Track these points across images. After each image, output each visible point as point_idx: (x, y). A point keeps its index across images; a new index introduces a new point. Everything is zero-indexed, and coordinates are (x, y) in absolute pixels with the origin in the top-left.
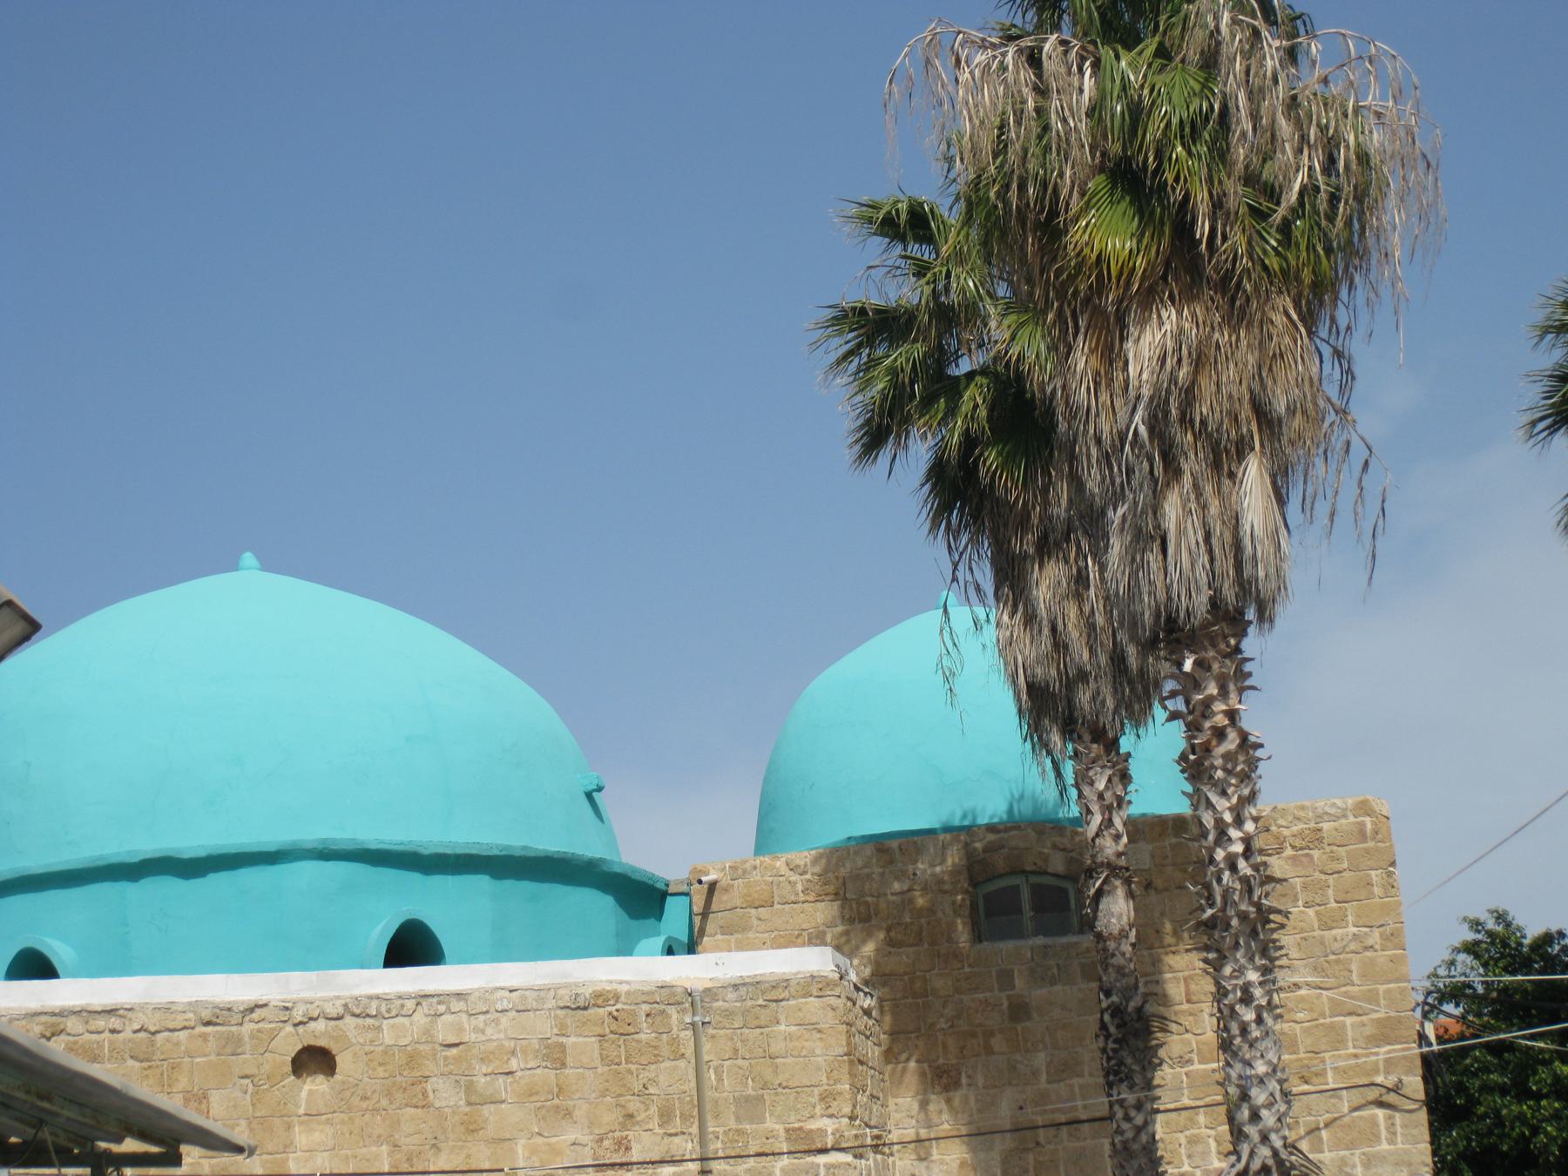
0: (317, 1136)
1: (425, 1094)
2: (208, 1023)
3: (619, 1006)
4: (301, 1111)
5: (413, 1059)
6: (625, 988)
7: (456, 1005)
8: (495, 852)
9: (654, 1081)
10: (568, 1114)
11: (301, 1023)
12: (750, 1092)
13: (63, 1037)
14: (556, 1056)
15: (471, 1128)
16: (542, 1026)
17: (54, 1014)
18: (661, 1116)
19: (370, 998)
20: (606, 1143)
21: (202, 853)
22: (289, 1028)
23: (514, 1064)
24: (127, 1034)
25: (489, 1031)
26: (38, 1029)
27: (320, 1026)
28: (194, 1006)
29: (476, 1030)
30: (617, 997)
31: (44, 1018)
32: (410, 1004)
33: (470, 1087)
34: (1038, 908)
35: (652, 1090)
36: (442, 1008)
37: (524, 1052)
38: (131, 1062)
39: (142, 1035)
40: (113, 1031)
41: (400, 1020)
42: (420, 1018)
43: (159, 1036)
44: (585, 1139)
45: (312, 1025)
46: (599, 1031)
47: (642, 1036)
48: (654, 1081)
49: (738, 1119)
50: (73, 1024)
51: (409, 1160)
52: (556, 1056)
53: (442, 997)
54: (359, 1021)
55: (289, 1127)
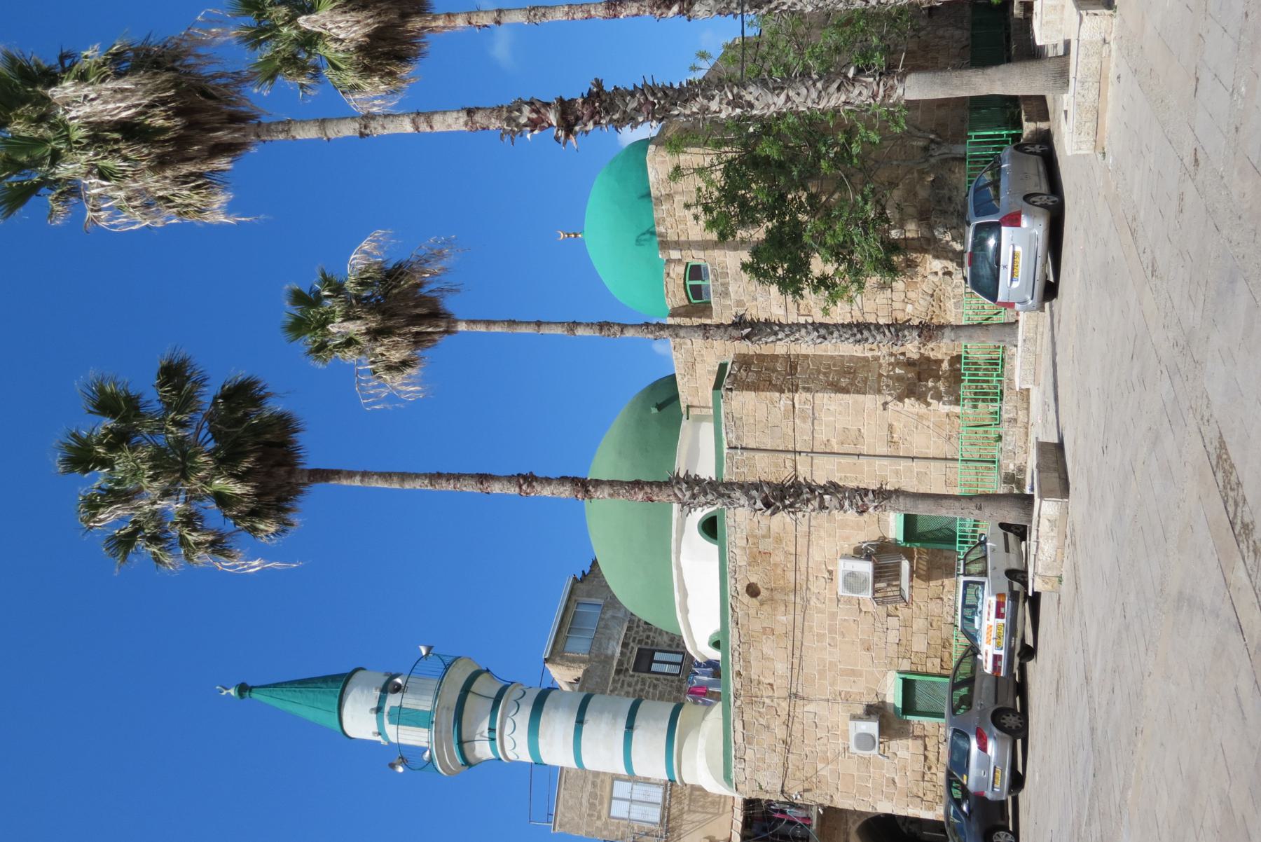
33: (764, 537)
34: (700, 278)
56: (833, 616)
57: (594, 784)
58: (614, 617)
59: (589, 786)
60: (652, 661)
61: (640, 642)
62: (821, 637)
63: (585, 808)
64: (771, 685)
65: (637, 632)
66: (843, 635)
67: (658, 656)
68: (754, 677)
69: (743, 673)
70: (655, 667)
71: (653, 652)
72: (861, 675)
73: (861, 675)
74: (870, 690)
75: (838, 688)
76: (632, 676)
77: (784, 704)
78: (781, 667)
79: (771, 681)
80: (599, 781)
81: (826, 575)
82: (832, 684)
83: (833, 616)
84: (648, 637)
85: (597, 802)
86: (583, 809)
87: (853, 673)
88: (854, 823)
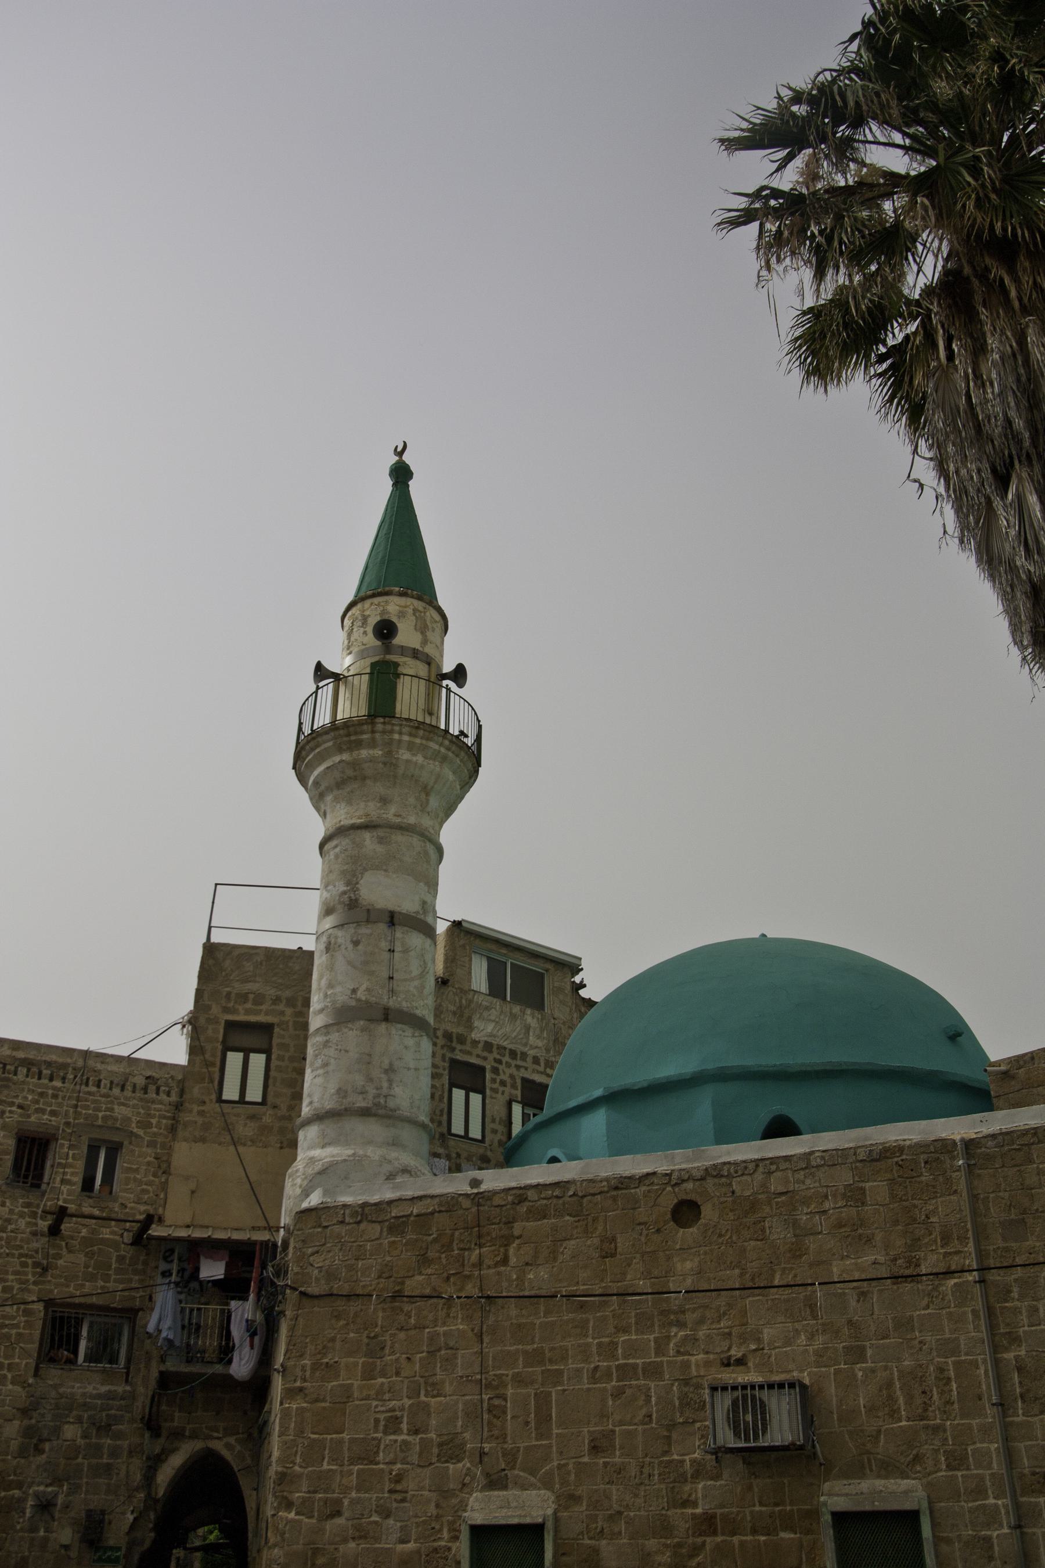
0: (688, 1265)
1: (763, 1230)
2: (616, 1188)
3: (904, 1157)
4: (678, 1247)
5: (754, 1205)
6: (908, 1143)
7: (783, 1165)
8: (844, 1067)
9: (934, 1212)
10: (869, 1240)
11: (676, 1184)
12: (1013, 1216)
13: (527, 1204)
14: (856, 1195)
15: (797, 1252)
16: (845, 1177)
17: (520, 1188)
18: (942, 1239)
19: (725, 1163)
20: (899, 1262)
21: (645, 1085)
22: (669, 1189)
23: (827, 1205)
24: (567, 1199)
25: (808, 1181)
26: (510, 1198)
27: (690, 1185)
28: (607, 1179)
29: (798, 1182)
30: (901, 1149)
31: (514, 1192)
32: (751, 1166)
33: (795, 1224)
35: (932, 1220)
36: (773, 1167)
37: (834, 1196)
38: (568, 1218)
39: (575, 1198)
40: (557, 1197)
41: (745, 1178)
42: (759, 1176)
43: (585, 1200)
44: (881, 1259)
45: (685, 1185)
46: (889, 1176)
47: (923, 1178)
48: (934, 1212)
49: (1005, 1239)
50: (531, 1194)
51: (753, 1279)
52: (856, 1195)
53: (773, 1160)
54: (716, 1180)
55: (669, 1258)
56: (653, 1371)
57: (277, 1000)
58: (528, 1028)
59: (272, 992)
60: (468, 1090)
61: (495, 1071)
62: (609, 1350)
63: (238, 987)
64: (505, 1261)
65: (508, 1065)
66: (618, 1393)
67: (476, 1099)
68: (517, 1228)
69: (523, 1209)
70: (458, 1095)
71: (481, 1091)
72: (540, 1436)
73: (540, 1436)
74: (511, 1457)
75: (510, 1391)
76: (444, 1056)
77: (471, 1289)
78: (539, 1278)
79: (513, 1260)
80: (281, 1007)
81: (736, 1353)
82: (520, 1380)
83: (653, 1371)
84: (503, 1083)
85: (249, 1005)
86: (237, 985)
87: (544, 1419)
88: (228, 1446)
